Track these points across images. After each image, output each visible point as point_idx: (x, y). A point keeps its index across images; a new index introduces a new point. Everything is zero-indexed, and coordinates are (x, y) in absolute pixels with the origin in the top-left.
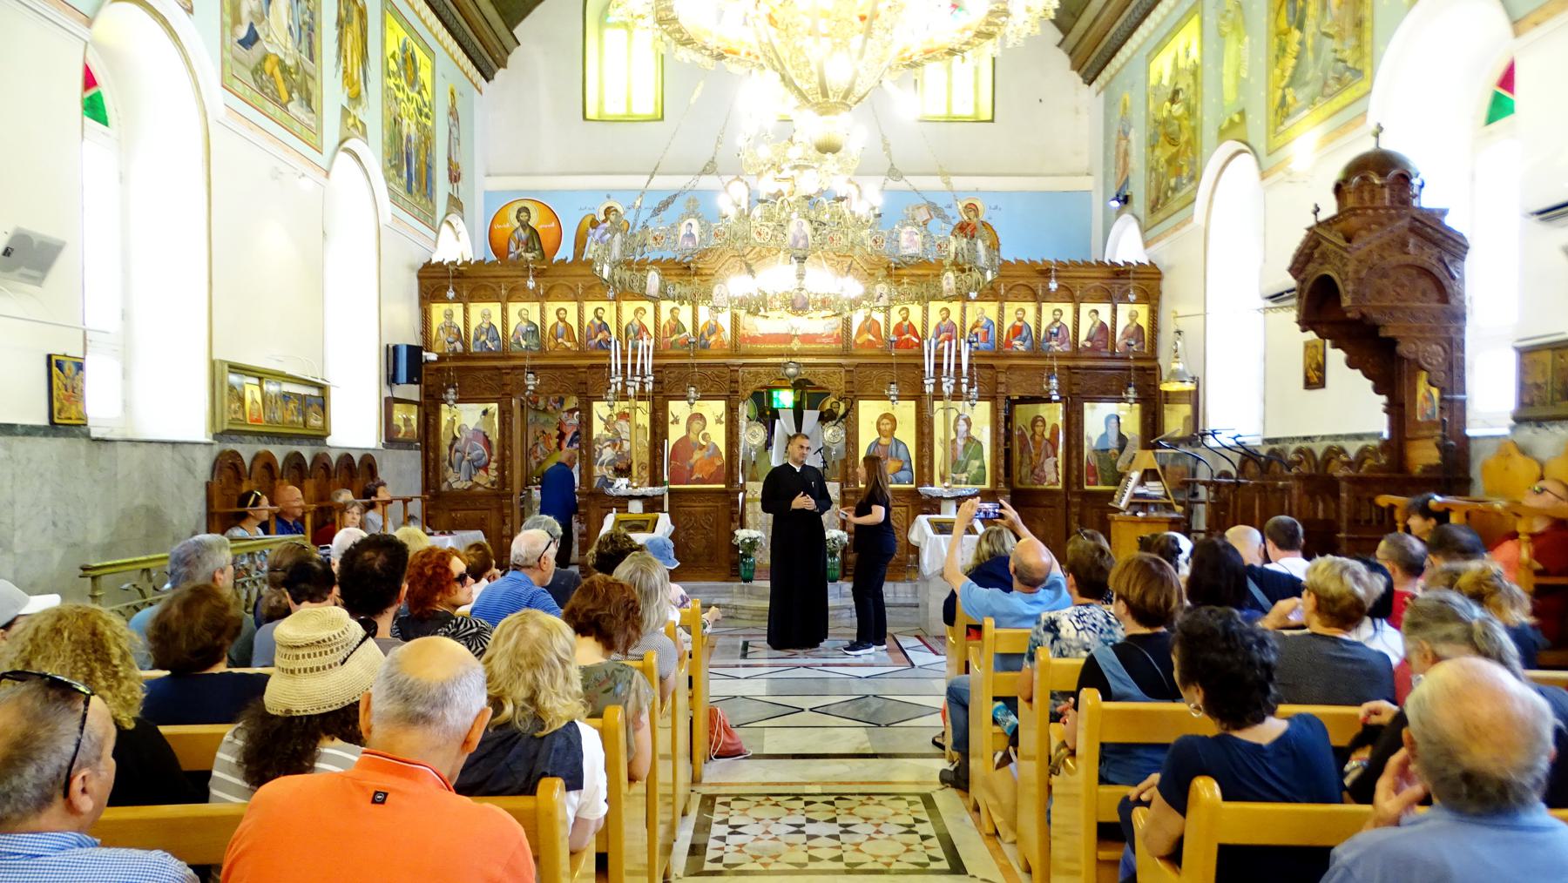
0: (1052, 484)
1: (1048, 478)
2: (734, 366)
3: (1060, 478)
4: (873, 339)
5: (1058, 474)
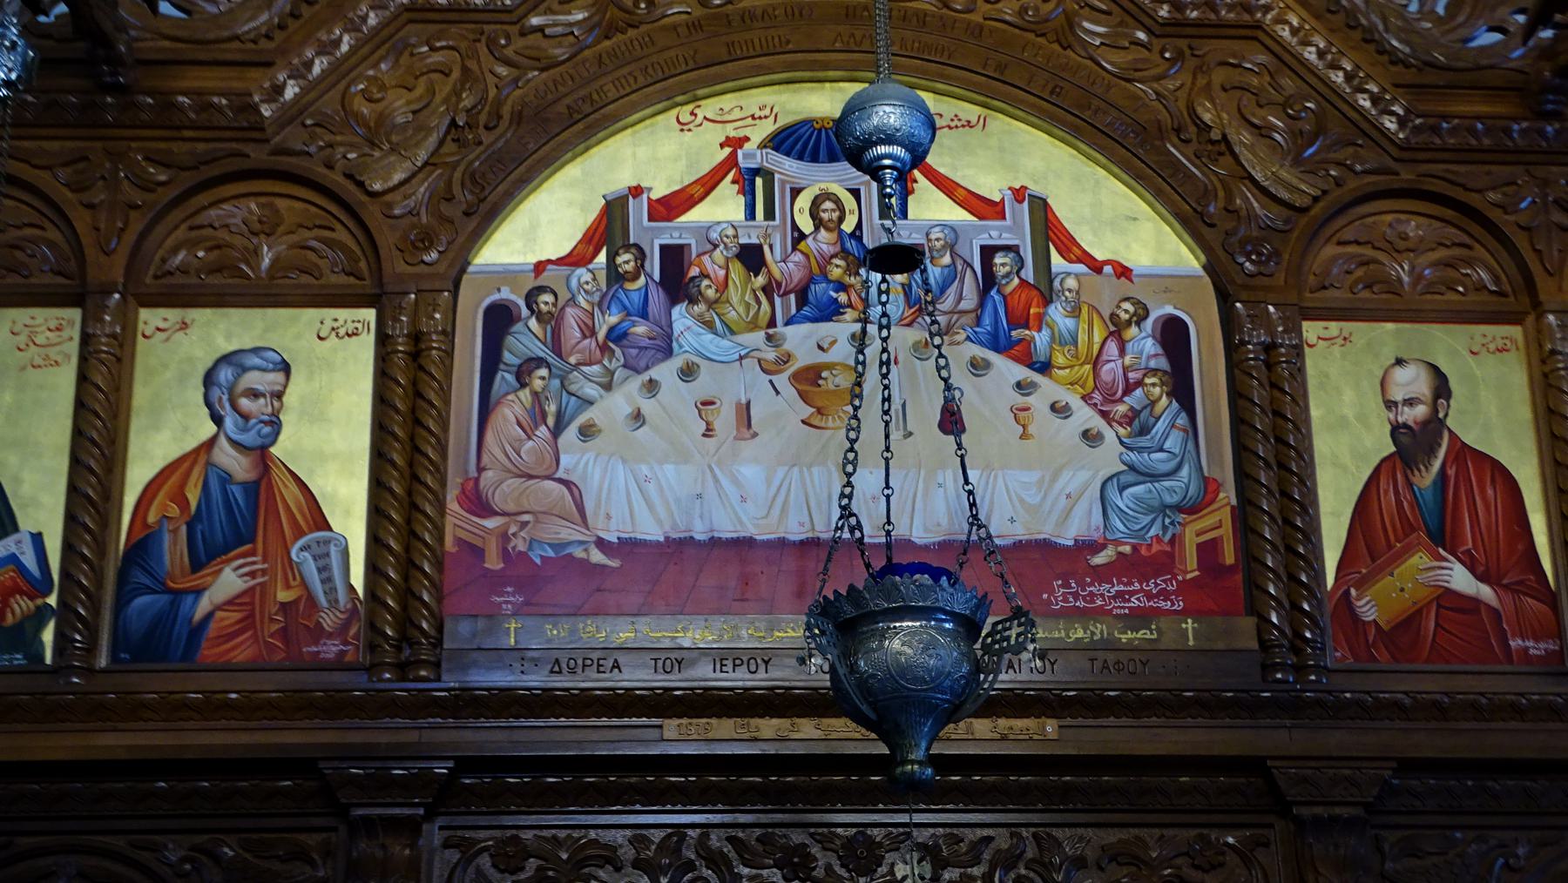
2: (383, 786)
4: (1486, 592)
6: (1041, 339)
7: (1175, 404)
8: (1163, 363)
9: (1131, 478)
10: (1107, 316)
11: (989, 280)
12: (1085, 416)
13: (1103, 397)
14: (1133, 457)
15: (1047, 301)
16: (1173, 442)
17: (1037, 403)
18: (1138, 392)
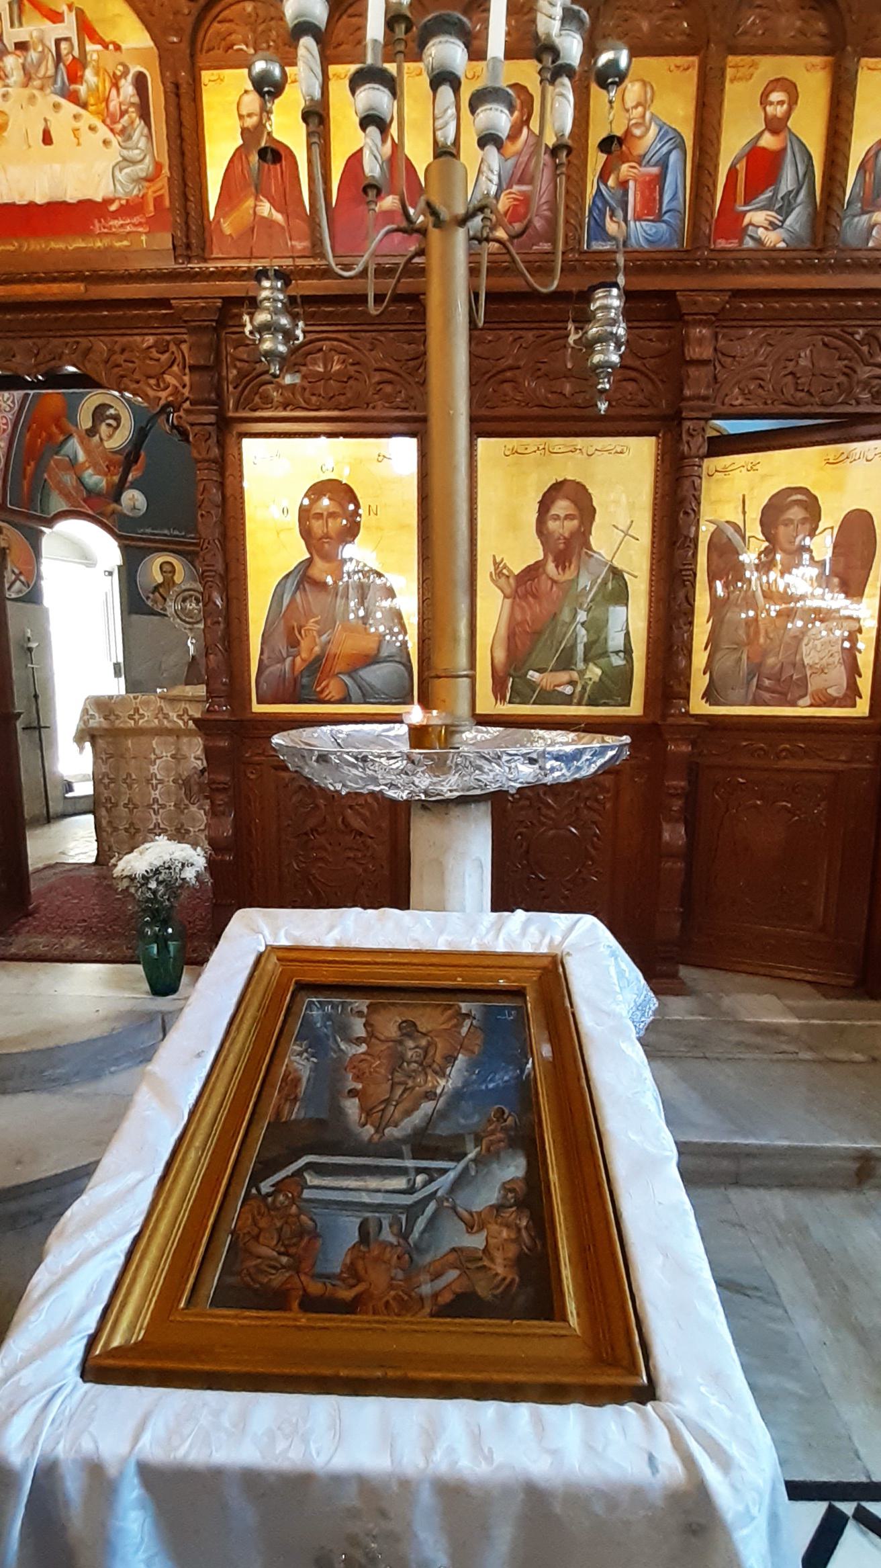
0: (831, 702)
1: (814, 684)
3: (865, 684)
4: (278, 217)
5: (854, 670)
6: (82, 89)
7: (142, 123)
8: (136, 100)
9: (126, 164)
10: (111, 74)
11: (59, 58)
12: (104, 132)
13: (110, 119)
14: (125, 153)
15: (84, 67)
16: (143, 143)
17: (83, 125)
18: (126, 117)
